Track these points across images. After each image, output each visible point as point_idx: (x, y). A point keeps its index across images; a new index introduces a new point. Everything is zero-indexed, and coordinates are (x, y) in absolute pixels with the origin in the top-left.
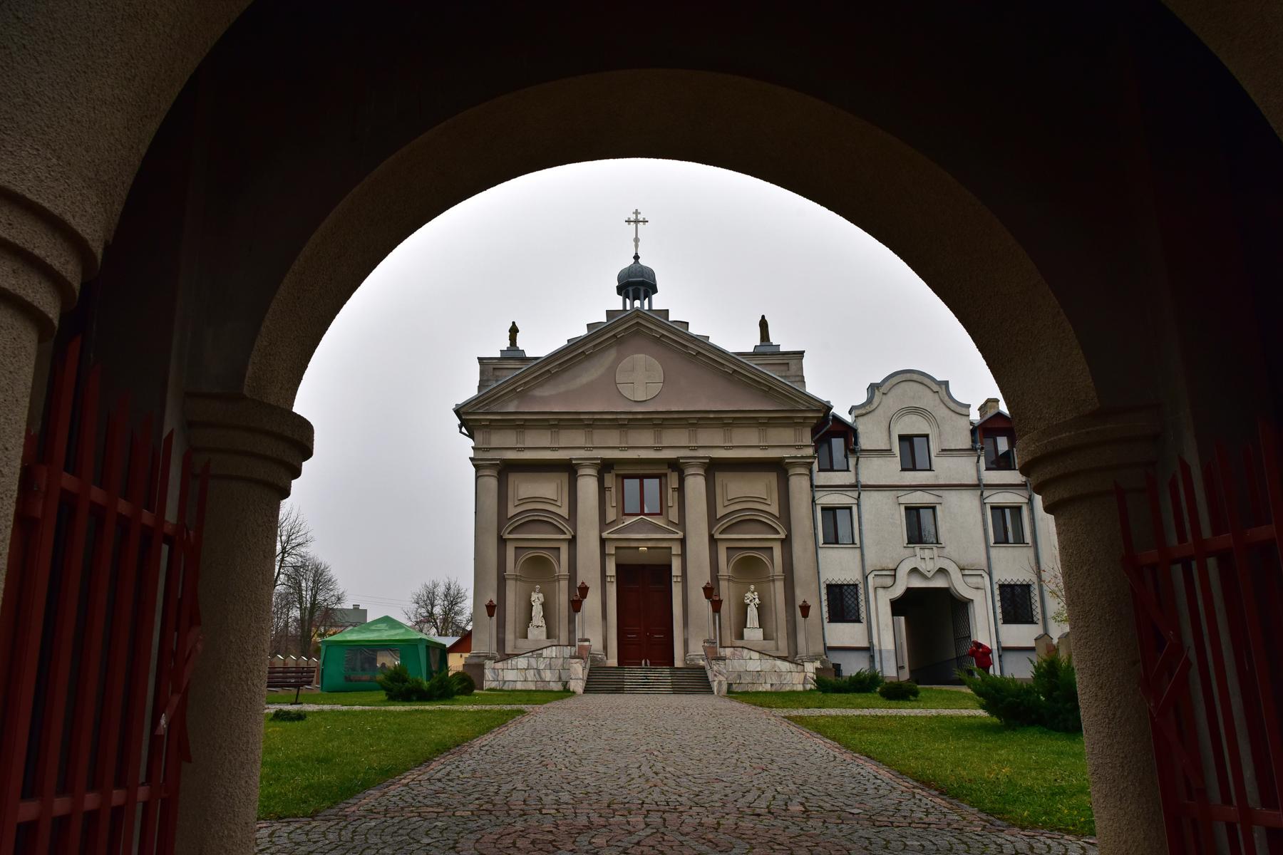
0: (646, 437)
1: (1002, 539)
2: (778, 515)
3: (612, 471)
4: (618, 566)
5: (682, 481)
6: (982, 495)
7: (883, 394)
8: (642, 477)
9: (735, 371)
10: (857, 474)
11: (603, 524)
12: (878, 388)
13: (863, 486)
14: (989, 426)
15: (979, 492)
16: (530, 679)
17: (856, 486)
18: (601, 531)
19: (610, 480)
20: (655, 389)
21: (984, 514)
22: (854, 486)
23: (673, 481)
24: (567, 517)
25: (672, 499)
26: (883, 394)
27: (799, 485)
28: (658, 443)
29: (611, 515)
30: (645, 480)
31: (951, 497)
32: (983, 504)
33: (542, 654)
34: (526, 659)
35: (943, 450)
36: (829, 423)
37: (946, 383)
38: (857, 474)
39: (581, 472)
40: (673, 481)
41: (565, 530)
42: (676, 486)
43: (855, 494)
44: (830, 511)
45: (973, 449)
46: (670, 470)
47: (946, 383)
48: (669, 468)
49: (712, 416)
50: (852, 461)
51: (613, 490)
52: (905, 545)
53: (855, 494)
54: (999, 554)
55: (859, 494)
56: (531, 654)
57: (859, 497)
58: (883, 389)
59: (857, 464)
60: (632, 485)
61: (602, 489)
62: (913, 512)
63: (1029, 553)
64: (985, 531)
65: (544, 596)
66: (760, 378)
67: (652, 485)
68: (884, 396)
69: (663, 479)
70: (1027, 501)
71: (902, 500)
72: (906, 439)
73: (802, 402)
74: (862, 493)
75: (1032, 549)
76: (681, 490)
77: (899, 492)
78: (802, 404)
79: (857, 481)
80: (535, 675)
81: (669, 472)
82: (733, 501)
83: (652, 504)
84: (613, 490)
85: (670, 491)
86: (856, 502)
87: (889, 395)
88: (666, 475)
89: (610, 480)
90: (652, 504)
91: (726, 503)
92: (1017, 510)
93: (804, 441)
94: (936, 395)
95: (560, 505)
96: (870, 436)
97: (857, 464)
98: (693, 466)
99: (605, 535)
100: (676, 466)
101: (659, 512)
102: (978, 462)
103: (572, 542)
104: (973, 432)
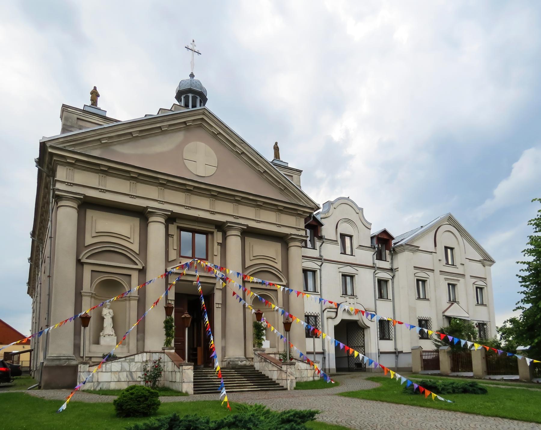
0: (203, 203)
1: (381, 296)
2: (281, 271)
3: (174, 223)
4: (175, 293)
5: (225, 238)
6: (374, 272)
7: (335, 208)
8: (194, 232)
9: (265, 172)
10: (320, 252)
11: (168, 261)
12: (332, 204)
13: (325, 260)
14: (380, 236)
15: (374, 270)
16: (123, 380)
17: (321, 259)
18: (166, 266)
19: (173, 229)
20: (211, 171)
21: (374, 283)
22: (320, 259)
23: (218, 237)
24: (138, 253)
25: (217, 249)
26: (335, 208)
27: (295, 252)
28: (212, 209)
29: (173, 255)
30: (196, 235)
31: (361, 270)
32: (375, 277)
33: (134, 359)
34: (120, 363)
35: (360, 246)
36: (311, 219)
37: (362, 209)
38: (320, 252)
39: (151, 219)
40: (218, 237)
41: (137, 262)
42: (220, 241)
43: (320, 263)
44: (305, 271)
45: (373, 247)
46: (216, 230)
47: (362, 209)
48: (216, 228)
49: (251, 197)
50: (318, 244)
51: (175, 237)
52: (341, 296)
53: (320, 263)
54: (381, 303)
55: (322, 263)
56: (124, 359)
57: (321, 265)
58: (335, 206)
59: (321, 246)
60: (186, 236)
61: (168, 235)
62: (344, 276)
63: (391, 304)
64: (375, 291)
65: (113, 311)
66: (281, 180)
67: (200, 239)
68: (335, 209)
69: (210, 237)
70: (391, 278)
71: (341, 270)
72: (343, 236)
73: (303, 201)
74: (324, 263)
75: (392, 303)
76: (223, 245)
77: (339, 265)
78: (303, 202)
79: (320, 256)
80: (127, 376)
81: (215, 231)
82: (256, 257)
83: (200, 252)
84: (175, 237)
85: (216, 244)
86: (319, 268)
87: (337, 209)
88: (212, 233)
89: (173, 229)
90: (200, 252)
91: (252, 258)
92: (386, 281)
93: (301, 226)
94: (357, 214)
95: (132, 242)
96: (328, 231)
97: (321, 246)
98: (236, 229)
99: (169, 269)
100: (222, 227)
101: (205, 258)
102: (374, 255)
103: (142, 271)
104: (372, 238)
